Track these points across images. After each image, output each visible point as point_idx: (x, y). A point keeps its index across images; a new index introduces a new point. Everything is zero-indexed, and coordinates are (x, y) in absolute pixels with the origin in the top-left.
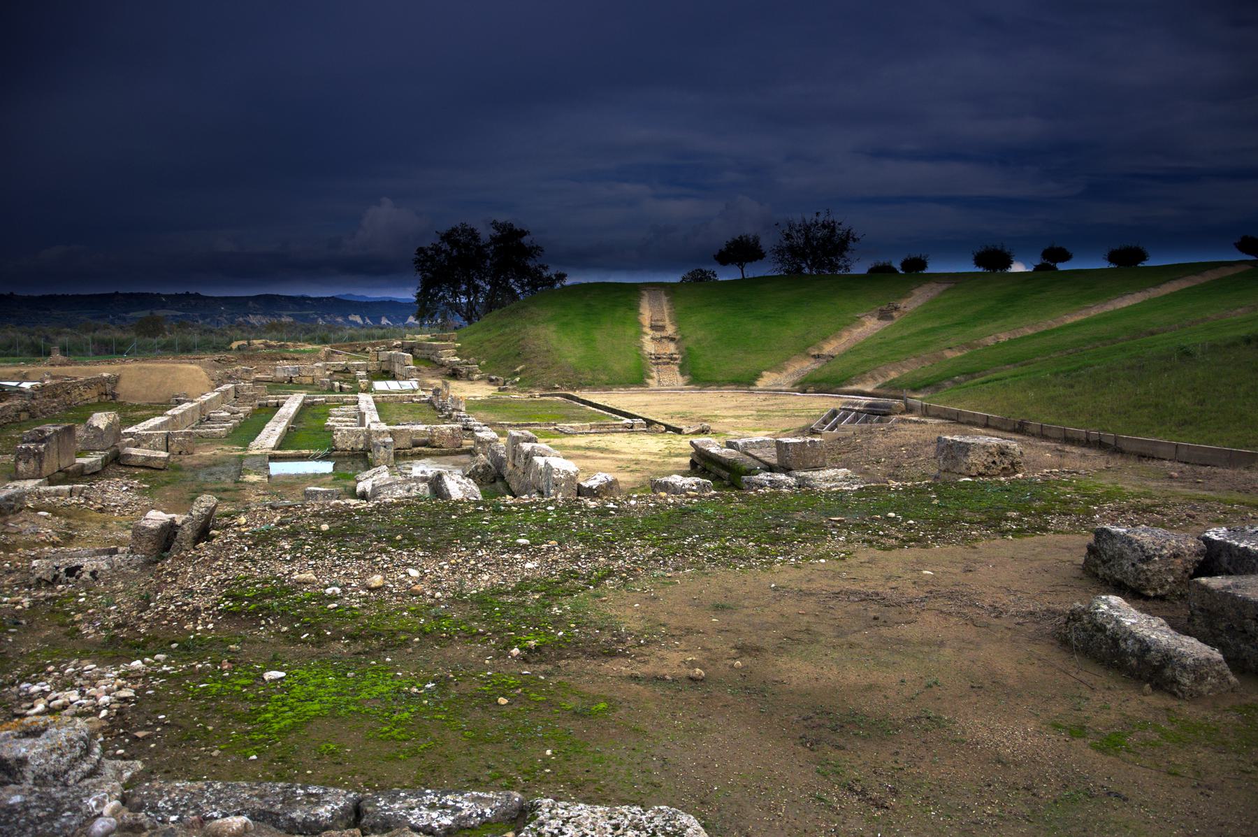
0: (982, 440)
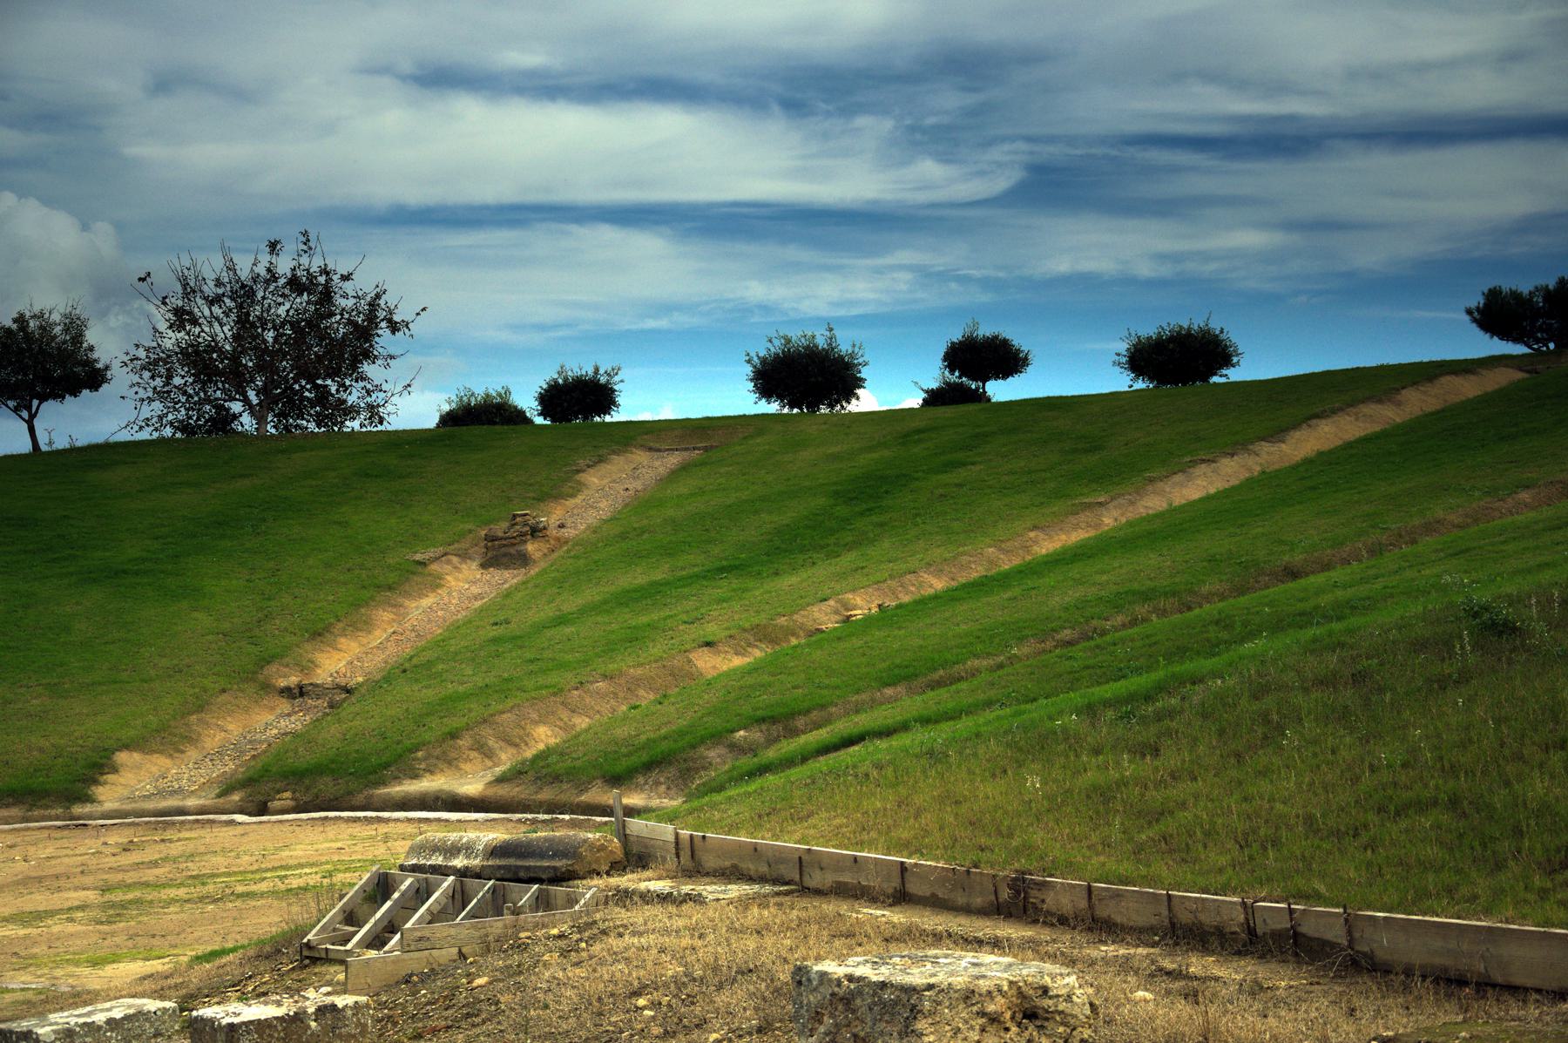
0: (954, 968)
